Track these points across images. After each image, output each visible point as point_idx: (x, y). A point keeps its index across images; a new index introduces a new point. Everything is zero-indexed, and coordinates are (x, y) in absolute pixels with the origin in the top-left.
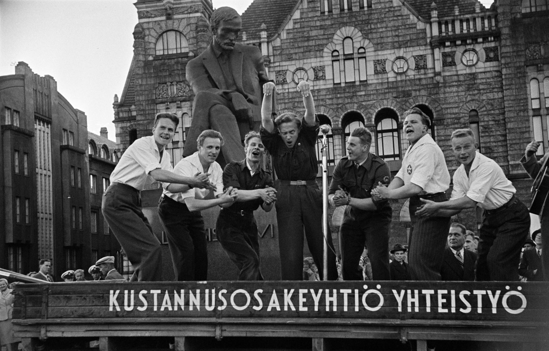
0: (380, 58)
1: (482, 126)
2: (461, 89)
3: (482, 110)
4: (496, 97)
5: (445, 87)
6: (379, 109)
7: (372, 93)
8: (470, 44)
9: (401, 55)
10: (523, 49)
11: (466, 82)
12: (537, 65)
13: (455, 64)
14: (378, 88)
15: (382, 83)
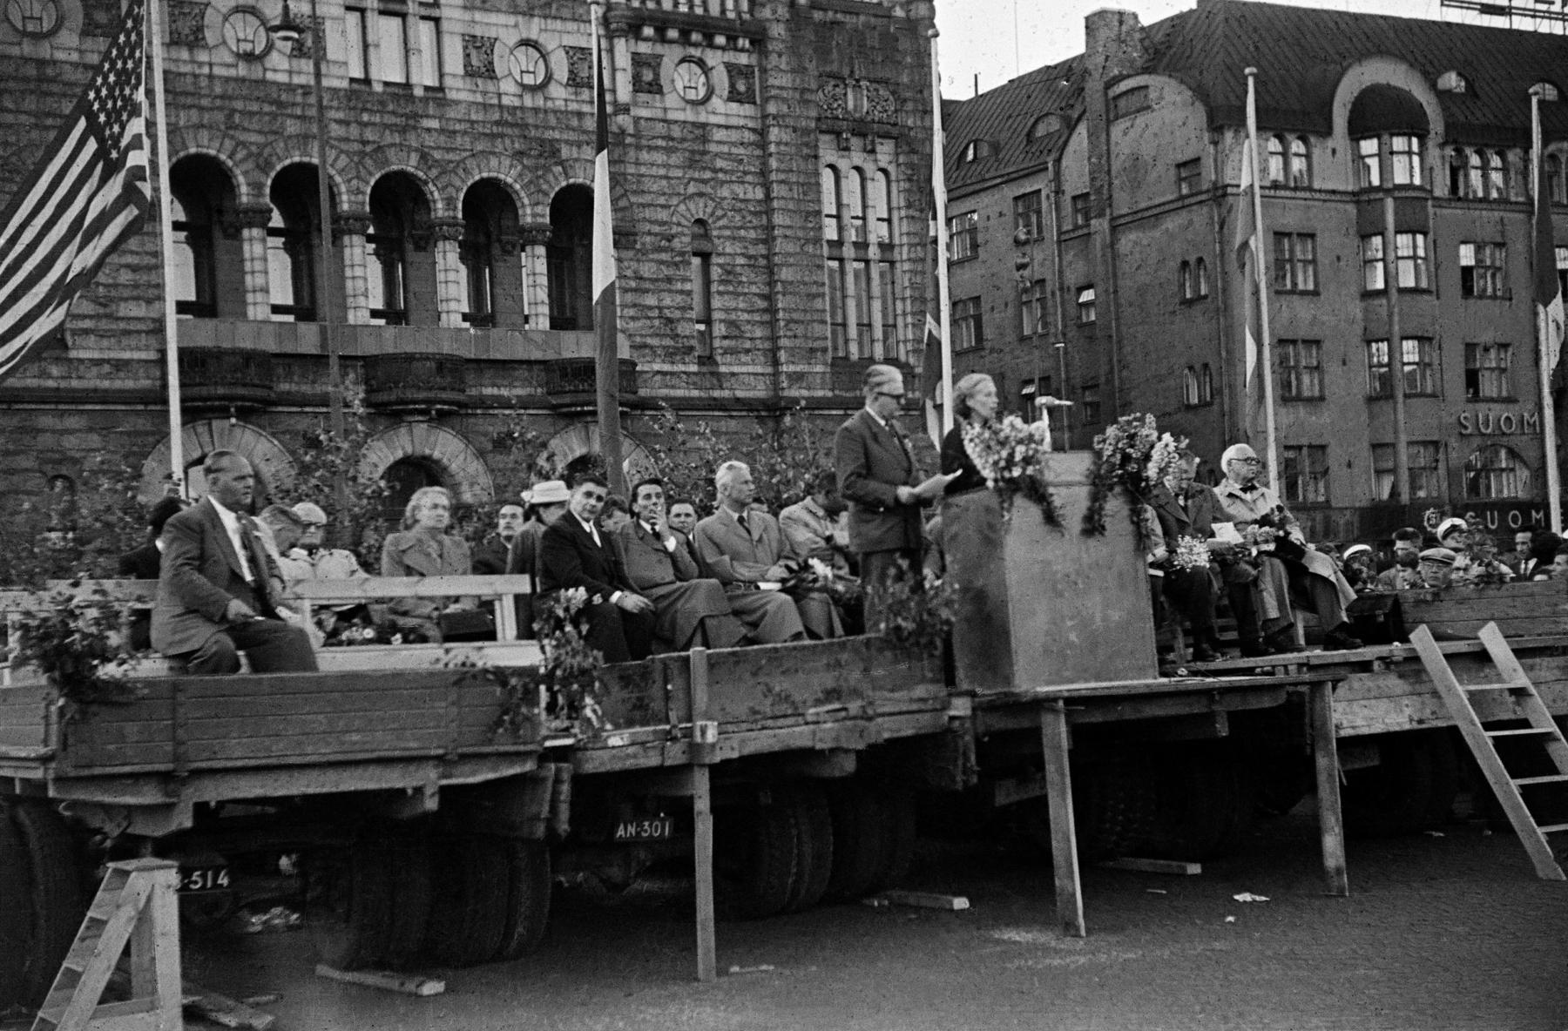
0: (478, 31)
1: (719, 265)
2: (675, 159)
3: (721, 223)
4: (750, 196)
5: (639, 148)
6: (477, 178)
7: (458, 127)
8: (696, 45)
9: (534, 36)
10: (814, 86)
11: (686, 145)
12: (838, 134)
13: (660, 91)
14: (474, 117)
15: (485, 107)
